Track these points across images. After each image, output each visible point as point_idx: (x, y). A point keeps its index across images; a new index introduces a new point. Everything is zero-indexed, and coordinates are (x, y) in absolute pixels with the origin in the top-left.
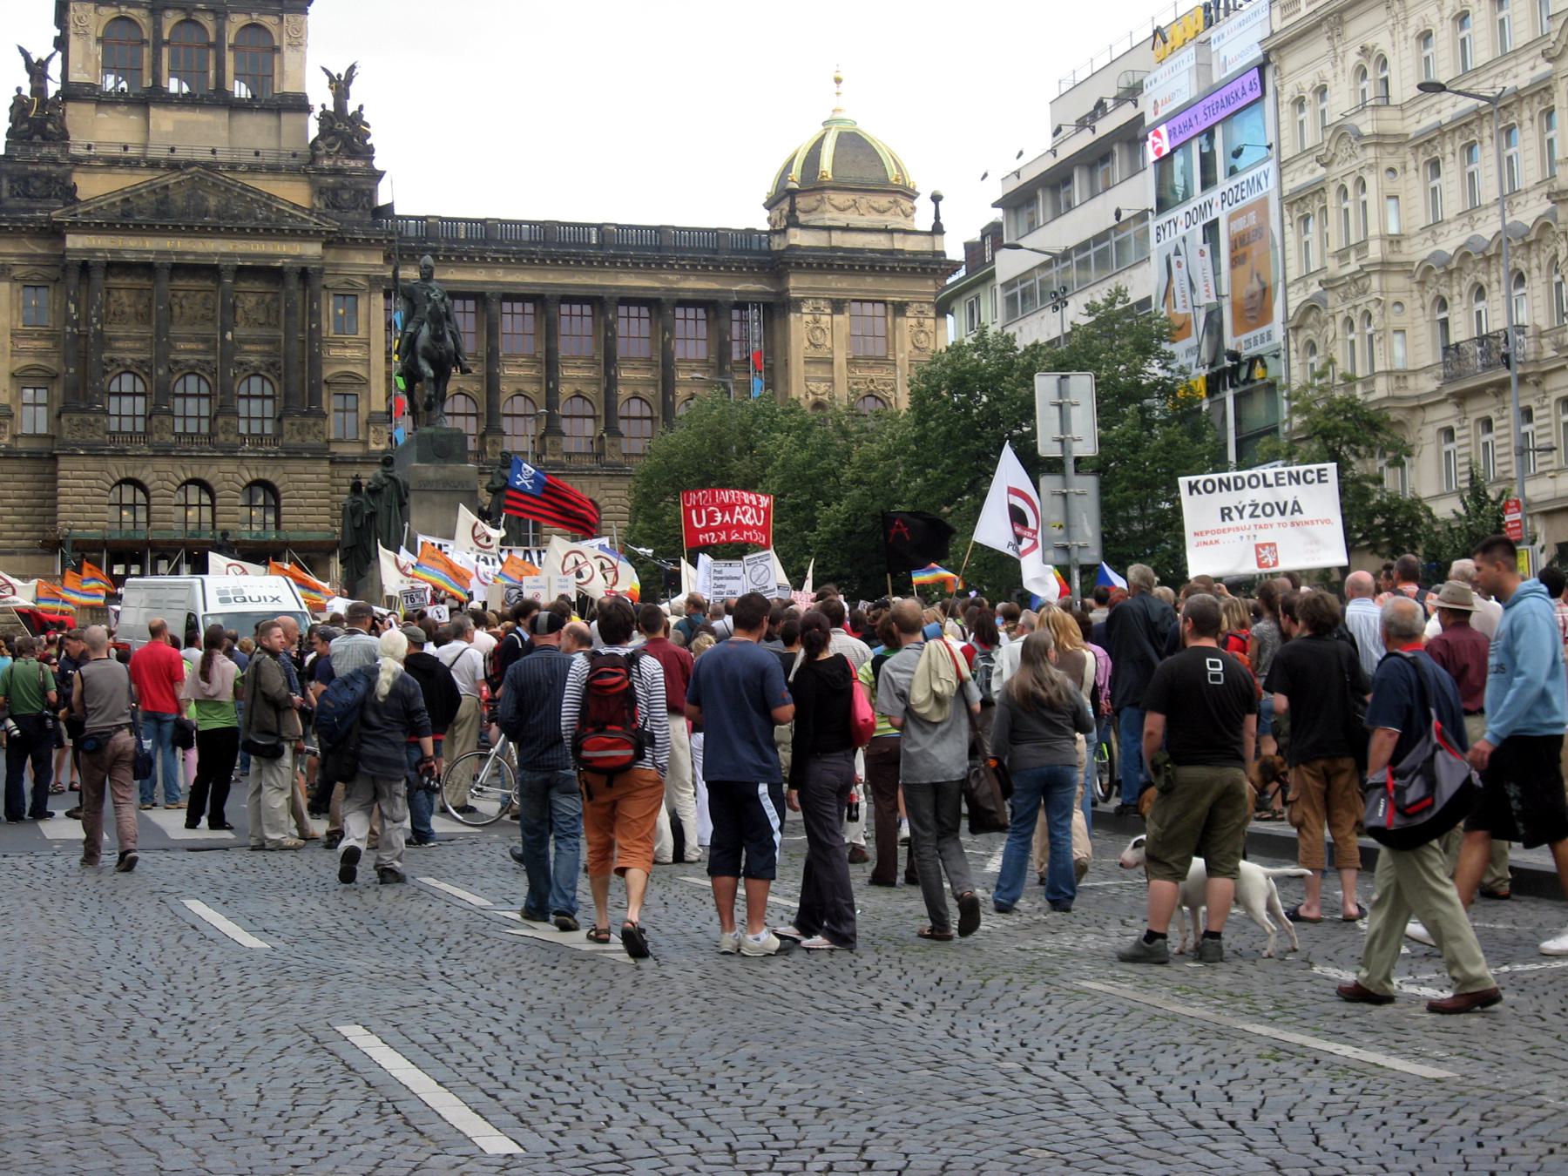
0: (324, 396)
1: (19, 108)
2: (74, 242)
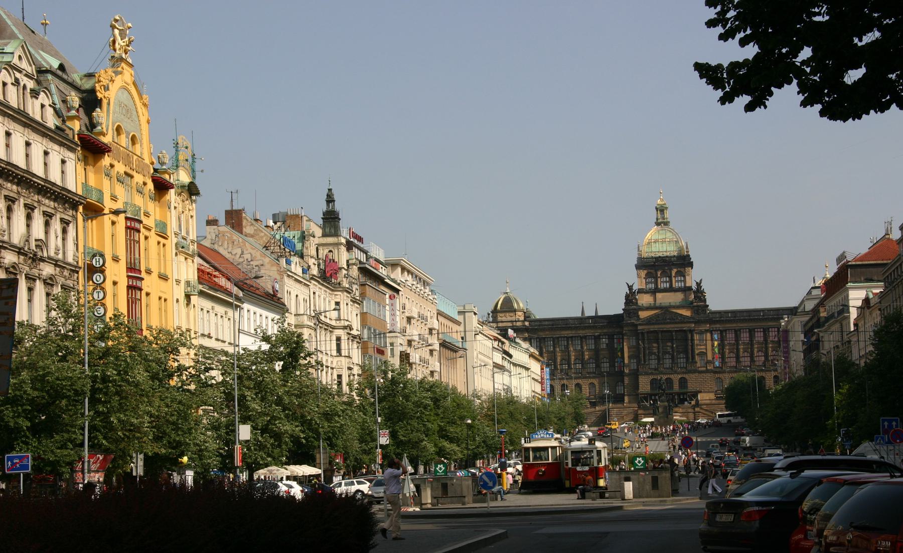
0: (696, 357)
1: (627, 297)
2: (640, 328)
